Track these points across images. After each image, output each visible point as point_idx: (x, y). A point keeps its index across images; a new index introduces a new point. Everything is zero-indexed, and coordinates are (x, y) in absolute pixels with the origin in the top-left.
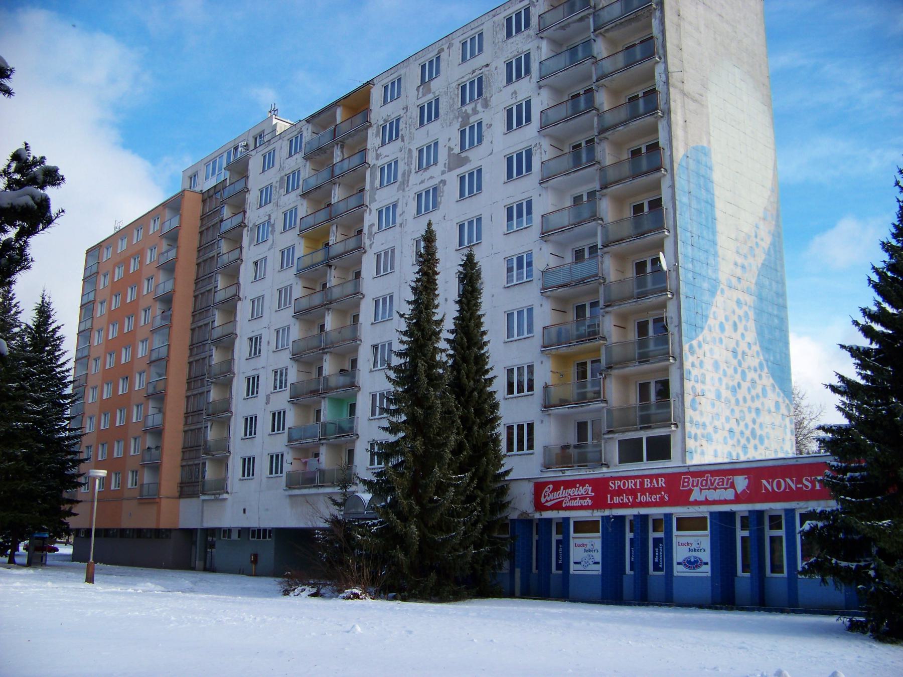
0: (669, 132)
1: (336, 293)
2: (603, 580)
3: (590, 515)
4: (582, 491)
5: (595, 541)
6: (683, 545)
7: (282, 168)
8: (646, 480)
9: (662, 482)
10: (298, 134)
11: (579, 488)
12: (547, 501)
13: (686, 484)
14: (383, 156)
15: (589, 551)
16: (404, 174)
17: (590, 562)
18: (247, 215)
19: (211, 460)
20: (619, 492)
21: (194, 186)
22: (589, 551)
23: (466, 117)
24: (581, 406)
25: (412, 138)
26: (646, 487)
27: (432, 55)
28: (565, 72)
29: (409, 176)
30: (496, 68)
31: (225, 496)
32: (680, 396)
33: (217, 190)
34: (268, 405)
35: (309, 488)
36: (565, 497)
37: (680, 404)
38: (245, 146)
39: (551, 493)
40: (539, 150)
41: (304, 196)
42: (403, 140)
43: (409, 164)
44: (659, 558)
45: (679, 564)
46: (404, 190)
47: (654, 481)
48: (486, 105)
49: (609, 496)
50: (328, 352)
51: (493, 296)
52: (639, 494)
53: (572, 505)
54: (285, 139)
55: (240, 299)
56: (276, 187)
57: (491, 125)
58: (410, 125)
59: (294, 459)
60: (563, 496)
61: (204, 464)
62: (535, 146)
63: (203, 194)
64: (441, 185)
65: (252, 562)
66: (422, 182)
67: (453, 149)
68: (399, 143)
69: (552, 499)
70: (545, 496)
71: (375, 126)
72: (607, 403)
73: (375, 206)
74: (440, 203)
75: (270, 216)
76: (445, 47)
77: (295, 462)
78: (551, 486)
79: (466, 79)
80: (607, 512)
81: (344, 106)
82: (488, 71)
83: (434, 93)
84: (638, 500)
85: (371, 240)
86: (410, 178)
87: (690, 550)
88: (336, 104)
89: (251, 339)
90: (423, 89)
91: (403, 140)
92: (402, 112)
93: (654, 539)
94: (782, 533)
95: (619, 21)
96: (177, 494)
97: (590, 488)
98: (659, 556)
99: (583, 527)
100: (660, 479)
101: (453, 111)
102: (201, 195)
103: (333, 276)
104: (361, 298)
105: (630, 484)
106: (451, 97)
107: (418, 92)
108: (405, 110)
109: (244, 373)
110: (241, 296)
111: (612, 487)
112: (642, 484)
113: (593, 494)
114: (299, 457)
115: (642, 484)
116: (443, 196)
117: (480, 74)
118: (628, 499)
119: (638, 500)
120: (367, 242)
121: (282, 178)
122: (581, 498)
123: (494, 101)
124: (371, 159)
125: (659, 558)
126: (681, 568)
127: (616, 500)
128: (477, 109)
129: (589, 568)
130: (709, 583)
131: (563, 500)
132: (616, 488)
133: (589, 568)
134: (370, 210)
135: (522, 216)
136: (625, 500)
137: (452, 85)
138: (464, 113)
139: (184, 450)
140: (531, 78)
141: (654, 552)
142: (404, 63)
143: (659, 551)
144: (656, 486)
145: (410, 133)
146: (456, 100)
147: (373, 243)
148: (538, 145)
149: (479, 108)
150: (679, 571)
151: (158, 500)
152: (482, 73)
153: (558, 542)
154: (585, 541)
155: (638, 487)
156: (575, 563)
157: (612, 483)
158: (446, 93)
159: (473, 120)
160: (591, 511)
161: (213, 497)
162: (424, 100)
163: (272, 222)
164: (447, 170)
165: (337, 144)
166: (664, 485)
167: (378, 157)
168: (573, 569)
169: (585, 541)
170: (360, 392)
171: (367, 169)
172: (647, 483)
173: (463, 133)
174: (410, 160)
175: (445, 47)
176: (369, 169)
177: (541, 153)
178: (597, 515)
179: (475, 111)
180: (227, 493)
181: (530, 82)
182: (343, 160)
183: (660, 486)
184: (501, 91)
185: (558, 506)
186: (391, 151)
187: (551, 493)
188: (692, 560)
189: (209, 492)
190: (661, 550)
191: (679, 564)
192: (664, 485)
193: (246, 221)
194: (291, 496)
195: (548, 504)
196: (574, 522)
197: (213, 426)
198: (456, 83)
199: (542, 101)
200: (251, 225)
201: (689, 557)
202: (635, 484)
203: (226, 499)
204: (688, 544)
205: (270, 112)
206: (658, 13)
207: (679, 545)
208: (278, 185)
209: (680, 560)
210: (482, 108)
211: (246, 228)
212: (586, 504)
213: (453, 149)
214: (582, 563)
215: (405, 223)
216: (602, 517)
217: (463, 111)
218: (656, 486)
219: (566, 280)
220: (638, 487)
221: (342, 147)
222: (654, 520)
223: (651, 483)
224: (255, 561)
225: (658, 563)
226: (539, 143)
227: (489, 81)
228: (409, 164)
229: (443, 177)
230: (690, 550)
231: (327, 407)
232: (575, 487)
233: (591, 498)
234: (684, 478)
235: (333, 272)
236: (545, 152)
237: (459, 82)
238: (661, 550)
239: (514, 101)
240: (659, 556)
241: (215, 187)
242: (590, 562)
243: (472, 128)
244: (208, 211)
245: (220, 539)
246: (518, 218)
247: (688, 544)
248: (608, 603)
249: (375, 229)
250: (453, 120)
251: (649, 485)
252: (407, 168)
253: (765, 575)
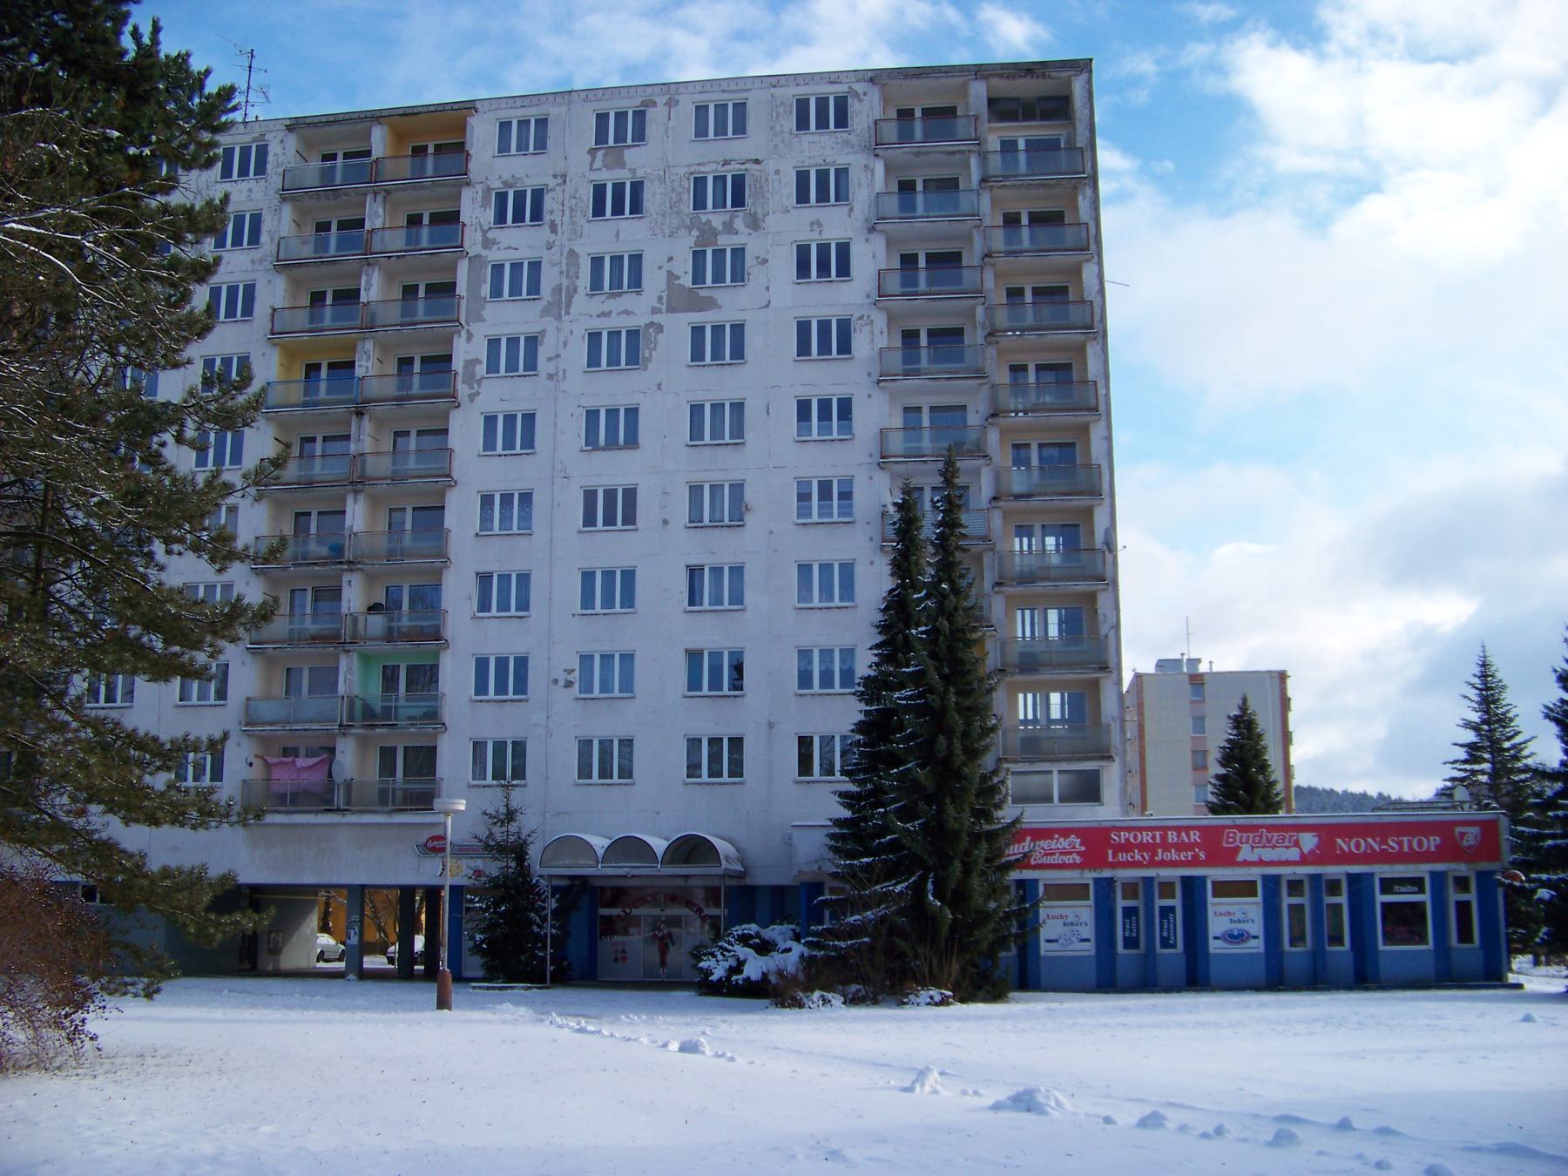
3: (1077, 876)
4: (1063, 843)
5: (1083, 912)
6: (1221, 915)
8: (1170, 833)
9: (1195, 836)
10: (252, 142)
11: (1058, 839)
13: (1231, 840)
15: (1072, 924)
16: (557, 290)
17: (1074, 939)
22: (1072, 924)
23: (708, 234)
25: (576, 233)
26: (1170, 841)
27: (629, 105)
29: (570, 297)
30: (777, 172)
32: (1118, 721)
35: (317, 812)
40: (868, 328)
42: (553, 228)
45: (1216, 938)
46: (559, 318)
47: (1183, 834)
48: (755, 224)
49: (1110, 852)
50: (361, 570)
51: (771, 532)
52: (1160, 851)
57: (765, 261)
58: (571, 209)
59: (256, 756)
62: (861, 318)
64: (651, 330)
67: (678, 278)
68: (544, 233)
71: (479, 188)
73: (481, 332)
74: (649, 359)
76: (661, 101)
80: (1106, 873)
83: (633, 171)
85: (471, 387)
87: (1232, 921)
88: (377, 117)
90: (604, 155)
91: (553, 228)
92: (552, 183)
97: (1078, 841)
98: (1168, 929)
100: (1191, 832)
105: (1146, 837)
107: (594, 158)
108: (560, 181)
112: (1164, 837)
113: (1083, 848)
115: (1164, 837)
118: (1142, 856)
120: (462, 390)
122: (1061, 854)
123: (771, 222)
124: (472, 241)
126: (1219, 943)
127: (1122, 857)
129: (1073, 947)
130: (1263, 962)
132: (1123, 842)
134: (470, 336)
136: (1138, 857)
137: (675, 170)
138: (705, 224)
140: (851, 210)
141: (1161, 924)
143: (1169, 923)
144: (1187, 840)
145: (574, 223)
146: (685, 197)
147: (478, 393)
149: (739, 224)
150: (1215, 947)
152: (746, 170)
156: (1048, 941)
159: (726, 241)
160: (1078, 871)
162: (609, 177)
164: (664, 308)
165: (375, 194)
167: (488, 243)
168: (1044, 948)
172: (1172, 837)
173: (698, 257)
175: (661, 101)
177: (872, 332)
178: (1089, 876)
179: (729, 228)
181: (849, 215)
183: (1192, 840)
184: (788, 211)
186: (518, 243)
191: (1216, 938)
196: (1045, 885)
198: (686, 169)
199: (873, 253)
201: (1232, 930)
202: (1154, 837)
204: (1229, 914)
206: (1088, 191)
212: (1071, 861)
213: (678, 278)
215: (561, 374)
217: (704, 221)
218: (1187, 840)
220: (1158, 841)
221: (384, 201)
223: (1178, 837)
225: (1168, 938)
226: (868, 317)
227: (761, 187)
229: (657, 319)
230: (1232, 921)
232: (1052, 839)
233: (1079, 853)
234: (1229, 833)
235: (367, 425)
237: (693, 169)
239: (815, 235)
240: (1168, 929)
242: (1074, 939)
243: (719, 254)
246: (820, 419)
247: (1229, 914)
249: (481, 370)
250: (679, 228)
252: (565, 282)
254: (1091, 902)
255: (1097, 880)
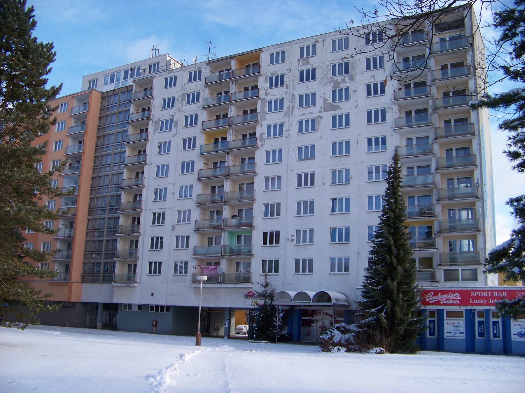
0: (477, 116)
1: (232, 170)
2: (466, 342)
3: (459, 308)
4: (453, 296)
5: (461, 322)
6: (516, 325)
7: (183, 88)
8: (494, 292)
9: (505, 294)
10: (197, 70)
11: (451, 294)
12: (430, 300)
13: (520, 296)
14: (271, 95)
15: (457, 326)
16: (289, 107)
17: (457, 332)
18: (152, 113)
19: (119, 261)
20: (474, 298)
21: (96, 87)
22: (457, 326)
23: (337, 84)
24: (423, 251)
25: (294, 88)
26: (495, 296)
27: (310, 43)
28: (461, 78)
29: (293, 110)
30: (359, 60)
31: (136, 284)
32: (484, 250)
33: (116, 92)
34: (174, 232)
35: (214, 283)
36: (442, 299)
37: (484, 254)
38: (144, 69)
39: (432, 296)
40: (391, 111)
41: (205, 108)
42: (287, 87)
43: (293, 102)
44: (496, 331)
45: (514, 335)
46: (289, 117)
47: (500, 293)
48: (352, 79)
49: (471, 299)
50: (227, 204)
51: (359, 186)
52: (490, 299)
53: (447, 303)
54: (186, 71)
55: (147, 164)
56: (178, 100)
57: (356, 91)
58: (293, 80)
59: (197, 265)
60: (441, 298)
61: (115, 263)
62: (389, 108)
63: (102, 93)
64: (319, 119)
65: (153, 325)
66: (304, 114)
67: (327, 100)
68: (284, 89)
69: (433, 299)
70: (428, 298)
71: (264, 76)
72: (438, 250)
73: (265, 123)
74: (318, 129)
75: (173, 116)
76: (320, 40)
77: (197, 267)
78: (433, 293)
79: (337, 62)
80: (469, 308)
81: (238, 60)
82: (353, 60)
83: (312, 65)
84: (490, 302)
85: (262, 142)
86: (294, 110)
87: (521, 328)
88: (232, 57)
89: (156, 190)
90: (303, 61)
91: (287, 87)
92: (286, 72)
93: (493, 322)
94: (435, 319)
95: (448, 52)
96: (80, 280)
97: (459, 295)
98: (496, 330)
99: (451, 314)
100: (503, 292)
101: (327, 78)
102: (101, 94)
103: (230, 160)
104: (256, 175)
105: (485, 294)
106: (325, 70)
107: (299, 62)
108: (289, 71)
109: (150, 210)
110: (147, 162)
111: (473, 295)
112: (492, 294)
113: (461, 298)
114: (199, 265)
115: (492, 294)
116: (320, 125)
117: (347, 61)
118: (484, 301)
119: (490, 302)
120: (259, 143)
121: (183, 95)
122: (452, 300)
123: (358, 78)
124: (262, 94)
125: (496, 331)
126: (516, 337)
127: (476, 301)
128: (346, 80)
129: (457, 335)
131: (441, 300)
132: (476, 296)
133: (457, 335)
134: (261, 125)
135: (379, 144)
136: (482, 302)
137: (326, 63)
138: (336, 80)
139: (86, 253)
140: (385, 70)
142: (287, 43)
143: (496, 328)
144: (501, 296)
145: (293, 85)
146: (329, 72)
147: (264, 144)
148: (390, 108)
149: (347, 79)
150: (514, 338)
151: (70, 284)
152: (349, 60)
153: (480, 323)
154: (454, 322)
155: (490, 296)
156: (447, 333)
157: (473, 293)
158: (321, 67)
159: (343, 86)
160: (459, 307)
161: (125, 285)
162: (304, 68)
163: (175, 120)
164: (323, 110)
165: (233, 82)
166: (506, 296)
167: (267, 94)
168: (446, 335)
169: (454, 322)
170: (255, 230)
171: (259, 100)
172: (495, 294)
173: (334, 92)
174: (293, 100)
175: (320, 40)
176: (260, 100)
177: (392, 113)
178: (463, 308)
179: (344, 81)
180: (137, 282)
181: (384, 72)
182: (235, 93)
183: (504, 296)
184: (363, 73)
185: (438, 303)
186: (277, 93)
187: (432, 296)
188: (523, 333)
189: (118, 282)
190: (498, 327)
191: (514, 335)
192: (506, 296)
193: (151, 116)
194: (194, 287)
195: (431, 302)
196: (446, 311)
197: (121, 240)
198: (329, 63)
199: (393, 85)
200: (155, 120)
202: (488, 294)
203: (135, 286)
204: (520, 325)
205: (153, 50)
206: (470, 53)
207: (514, 325)
208: (180, 98)
209: (515, 333)
210: (349, 80)
211: (152, 121)
212: (456, 303)
213: (327, 100)
214: (452, 333)
215: (290, 136)
216: (465, 310)
217: (335, 79)
218: (501, 296)
219: (412, 184)
220: (490, 296)
221: (236, 84)
222: (493, 312)
223: (498, 294)
224: (156, 325)
225: (496, 334)
226: (391, 107)
227: (354, 66)
228: (293, 102)
229: (320, 114)
230: (521, 328)
231: (226, 236)
232: (449, 294)
233: (459, 300)
234: (519, 293)
235: (231, 157)
236: (396, 112)
237: (331, 62)
238: (498, 327)
239: (372, 80)
240: (496, 330)
241: (114, 90)
242: (457, 332)
243: (340, 90)
244: (107, 105)
245: (148, 312)
246: (375, 145)
247: (520, 325)
248: (469, 353)
249: (265, 136)
250: (327, 83)
251: (497, 295)
252: (291, 105)
253: (511, 340)
254: (464, 318)
255: (466, 310)
